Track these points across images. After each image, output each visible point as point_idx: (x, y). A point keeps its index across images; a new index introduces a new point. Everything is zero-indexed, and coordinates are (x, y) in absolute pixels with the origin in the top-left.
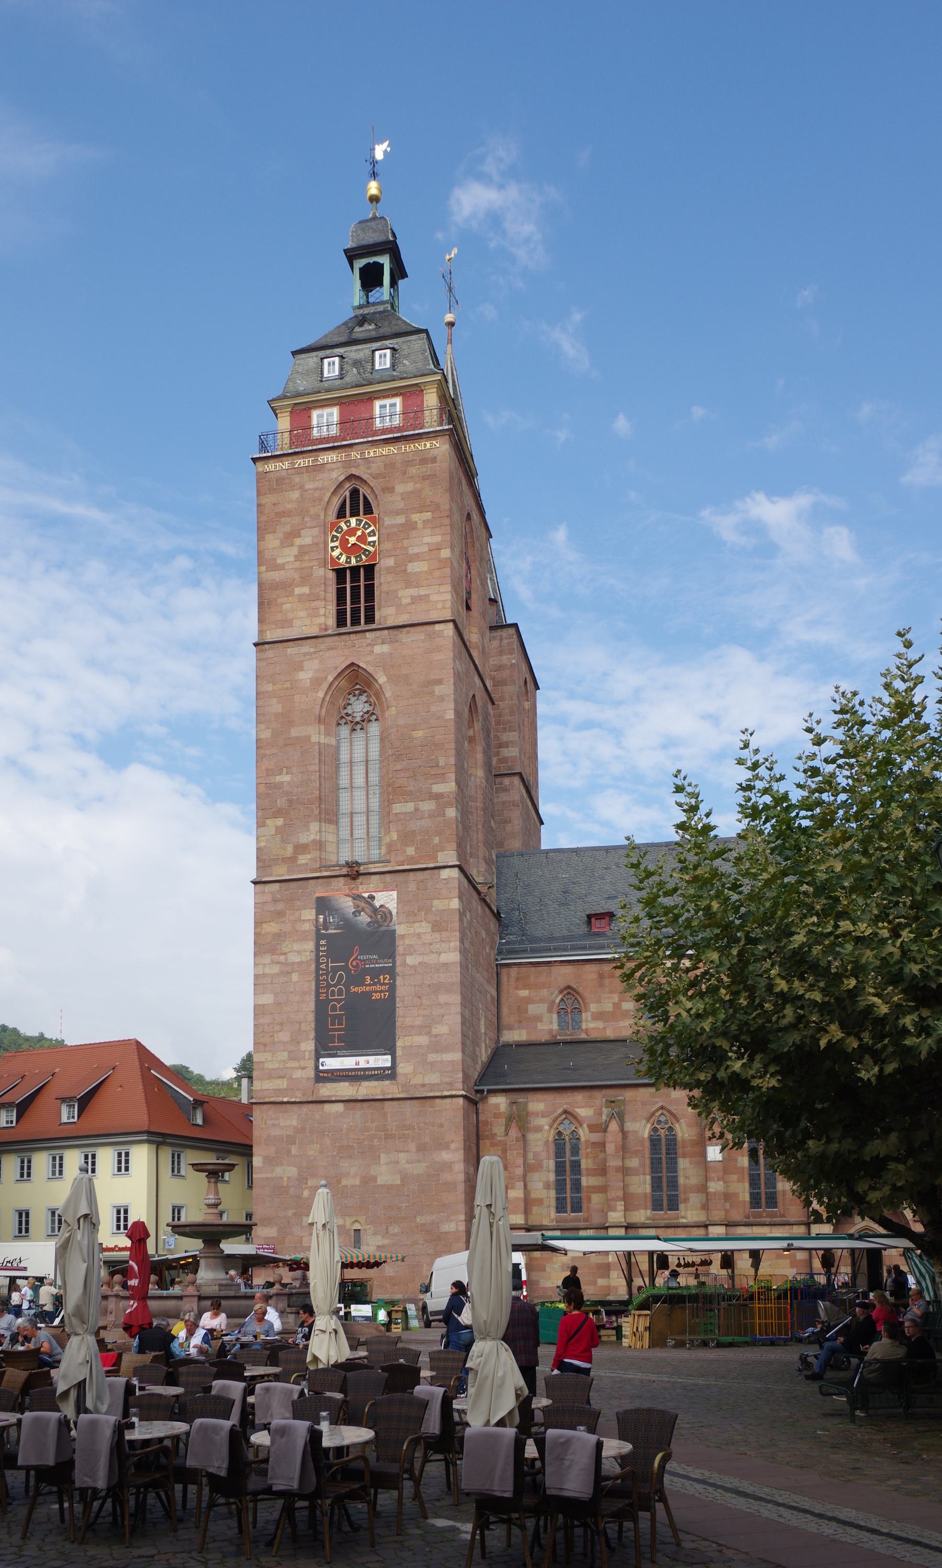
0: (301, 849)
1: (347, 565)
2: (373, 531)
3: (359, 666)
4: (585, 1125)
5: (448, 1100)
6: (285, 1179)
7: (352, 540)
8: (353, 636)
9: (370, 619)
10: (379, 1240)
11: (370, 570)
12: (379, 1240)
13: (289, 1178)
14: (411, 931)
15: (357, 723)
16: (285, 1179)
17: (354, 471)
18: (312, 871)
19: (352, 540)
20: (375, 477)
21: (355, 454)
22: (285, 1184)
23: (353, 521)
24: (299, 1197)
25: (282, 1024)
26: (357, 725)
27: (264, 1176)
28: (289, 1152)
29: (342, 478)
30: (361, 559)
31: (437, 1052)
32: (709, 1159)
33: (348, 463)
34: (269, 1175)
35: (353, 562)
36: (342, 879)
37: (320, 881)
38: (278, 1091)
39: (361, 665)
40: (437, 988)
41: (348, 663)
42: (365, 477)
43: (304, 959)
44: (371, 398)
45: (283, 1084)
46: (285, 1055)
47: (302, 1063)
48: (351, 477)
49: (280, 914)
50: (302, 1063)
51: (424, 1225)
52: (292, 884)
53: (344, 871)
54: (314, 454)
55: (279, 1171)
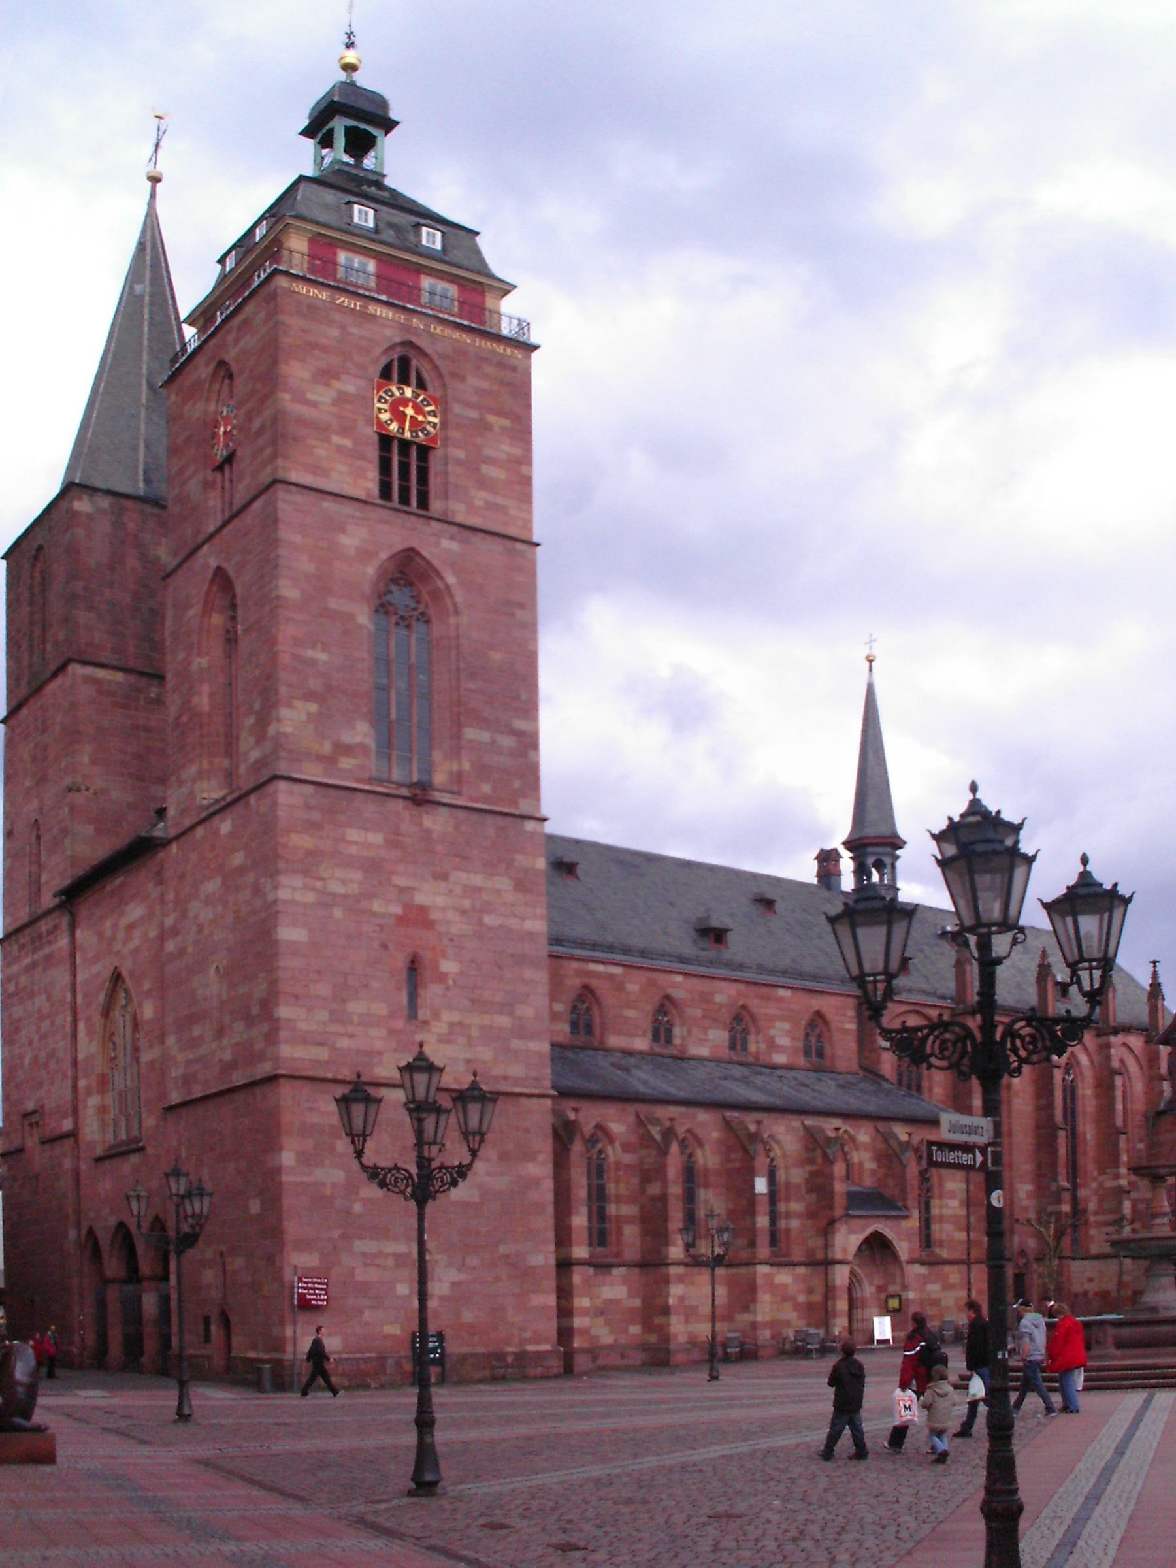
0: (346, 750)
1: (399, 436)
2: (433, 411)
3: (418, 554)
4: (617, 1143)
5: (535, 1100)
6: (329, 1185)
7: (410, 411)
8: (413, 519)
9: (424, 503)
10: (453, 1275)
11: (424, 451)
12: (453, 1275)
13: (334, 1185)
14: (489, 884)
15: (402, 618)
16: (329, 1185)
17: (414, 339)
18: (359, 781)
19: (410, 411)
20: (442, 356)
21: (415, 321)
22: (328, 1192)
23: (408, 392)
24: (348, 1212)
25: (319, 972)
26: (405, 622)
27: (298, 1179)
28: (332, 1149)
29: (398, 340)
30: (417, 436)
31: (521, 1038)
32: (757, 1192)
33: (407, 328)
34: (305, 1179)
35: (407, 435)
36: (401, 801)
37: (371, 796)
38: (316, 1063)
39: (425, 553)
40: (520, 960)
41: (406, 545)
42: (429, 351)
43: (350, 892)
44: (420, 270)
45: (323, 1054)
46: (323, 1015)
47: (350, 1029)
48: (409, 344)
49: (315, 826)
50: (350, 1029)
51: (507, 1256)
52: (332, 792)
53: (404, 792)
54: (365, 300)
55: (319, 1174)
